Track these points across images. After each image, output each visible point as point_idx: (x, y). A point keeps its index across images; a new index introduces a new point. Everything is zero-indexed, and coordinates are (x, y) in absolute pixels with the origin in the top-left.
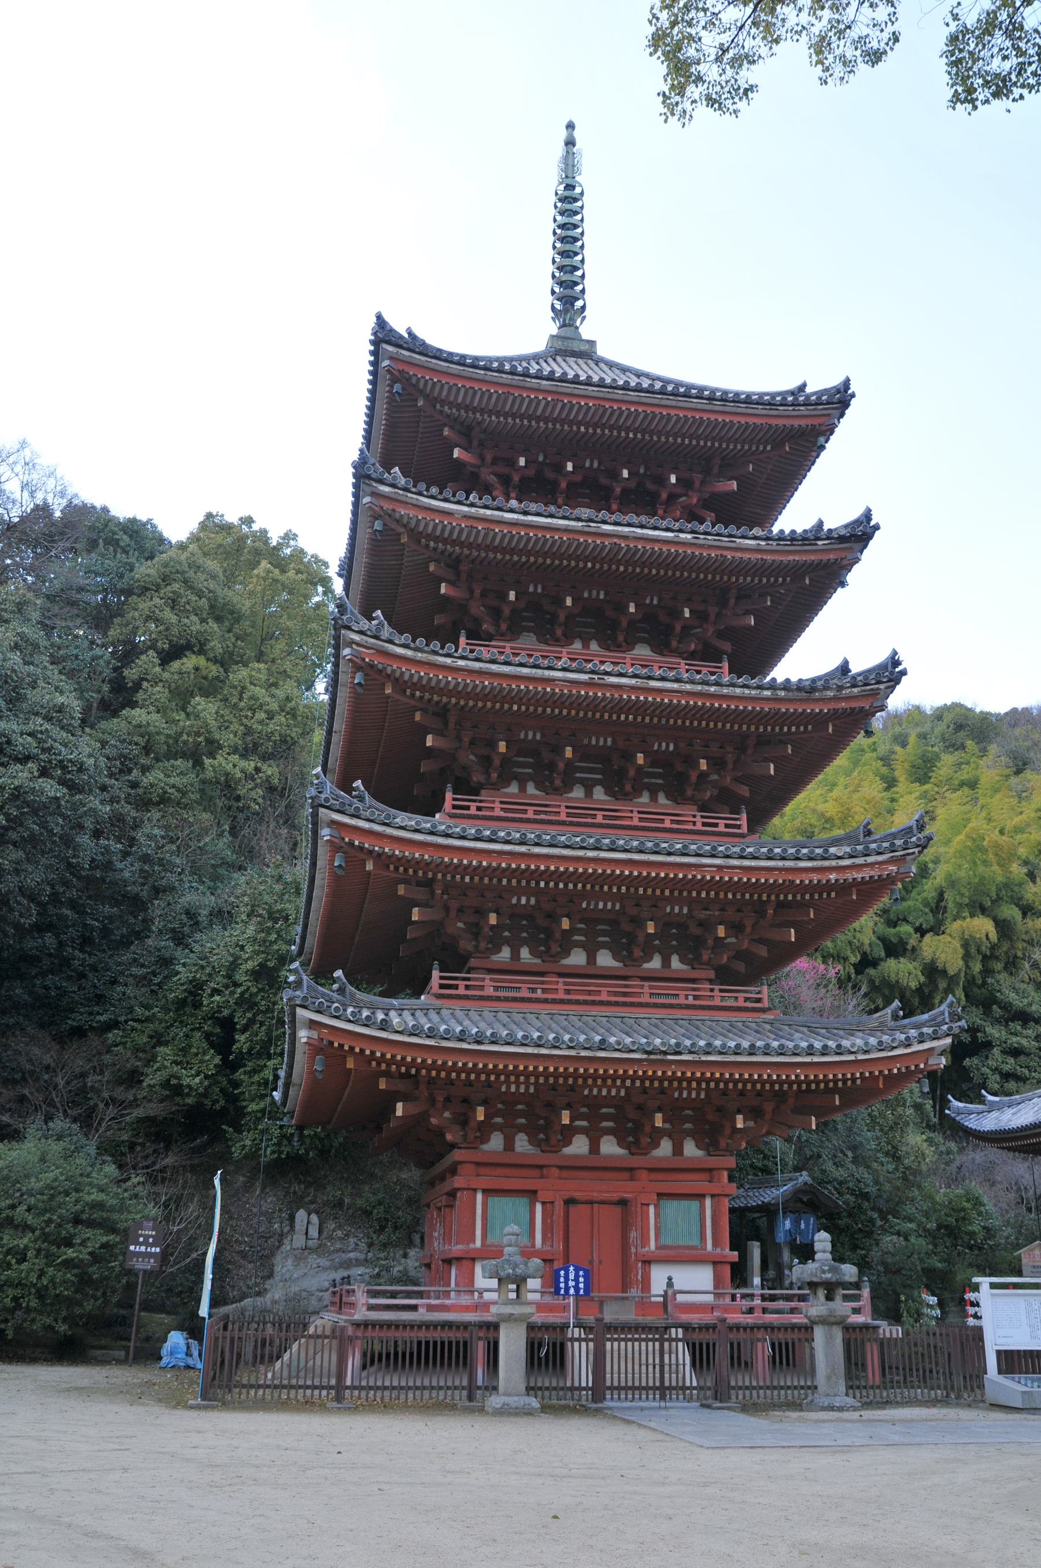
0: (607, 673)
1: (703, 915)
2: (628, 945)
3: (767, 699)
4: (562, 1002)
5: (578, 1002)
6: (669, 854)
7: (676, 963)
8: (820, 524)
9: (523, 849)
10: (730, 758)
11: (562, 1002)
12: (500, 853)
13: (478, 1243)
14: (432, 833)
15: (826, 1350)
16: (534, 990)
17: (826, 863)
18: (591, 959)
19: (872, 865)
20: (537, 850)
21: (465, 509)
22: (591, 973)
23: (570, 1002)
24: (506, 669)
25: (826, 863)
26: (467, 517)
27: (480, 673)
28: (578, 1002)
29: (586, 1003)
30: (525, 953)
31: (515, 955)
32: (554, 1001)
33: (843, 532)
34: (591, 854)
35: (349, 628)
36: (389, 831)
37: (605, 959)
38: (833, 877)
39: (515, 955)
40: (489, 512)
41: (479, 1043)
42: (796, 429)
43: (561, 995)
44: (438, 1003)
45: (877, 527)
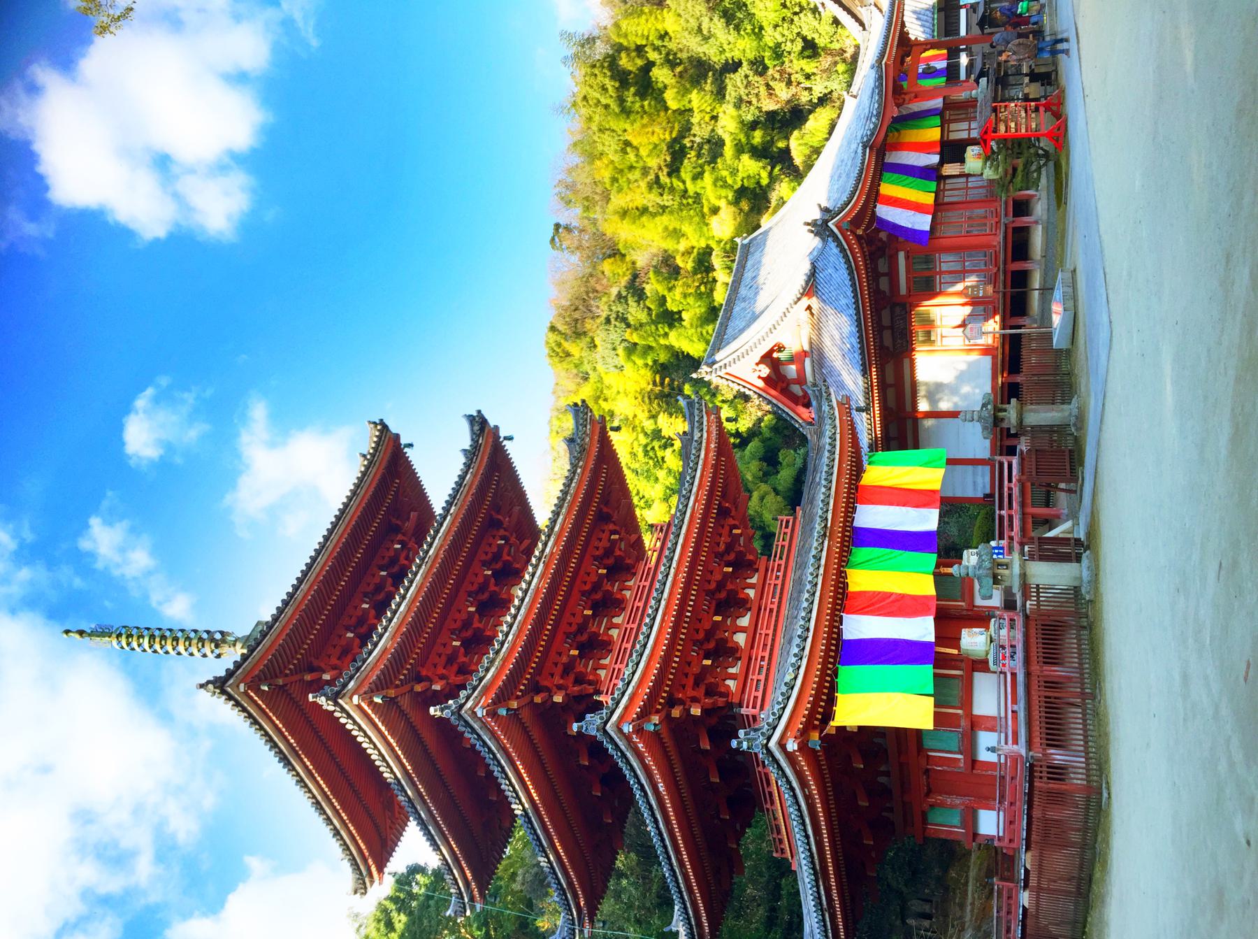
0: (543, 551)
1: (722, 547)
2: (732, 604)
3: (583, 473)
4: (775, 630)
5: (777, 621)
6: (683, 521)
7: (754, 580)
8: (465, 450)
9: (663, 603)
10: (612, 527)
11: (775, 630)
12: (663, 620)
13: (959, 711)
14: (641, 655)
15: (1041, 415)
16: (761, 667)
17: (704, 444)
18: (743, 630)
19: (709, 427)
20: (666, 595)
21: (387, 634)
22: (753, 632)
23: (776, 625)
24: (522, 611)
25: (704, 444)
26: (393, 637)
27: (520, 630)
28: (777, 621)
29: (778, 616)
30: (731, 670)
31: (733, 677)
32: (774, 635)
33: (476, 428)
34: (674, 564)
35: (462, 706)
36: (633, 684)
37: (744, 621)
38: (713, 446)
39: (733, 677)
40: (395, 620)
41: (808, 630)
42: (390, 468)
43: (770, 632)
44: (767, 707)
45: (479, 412)
